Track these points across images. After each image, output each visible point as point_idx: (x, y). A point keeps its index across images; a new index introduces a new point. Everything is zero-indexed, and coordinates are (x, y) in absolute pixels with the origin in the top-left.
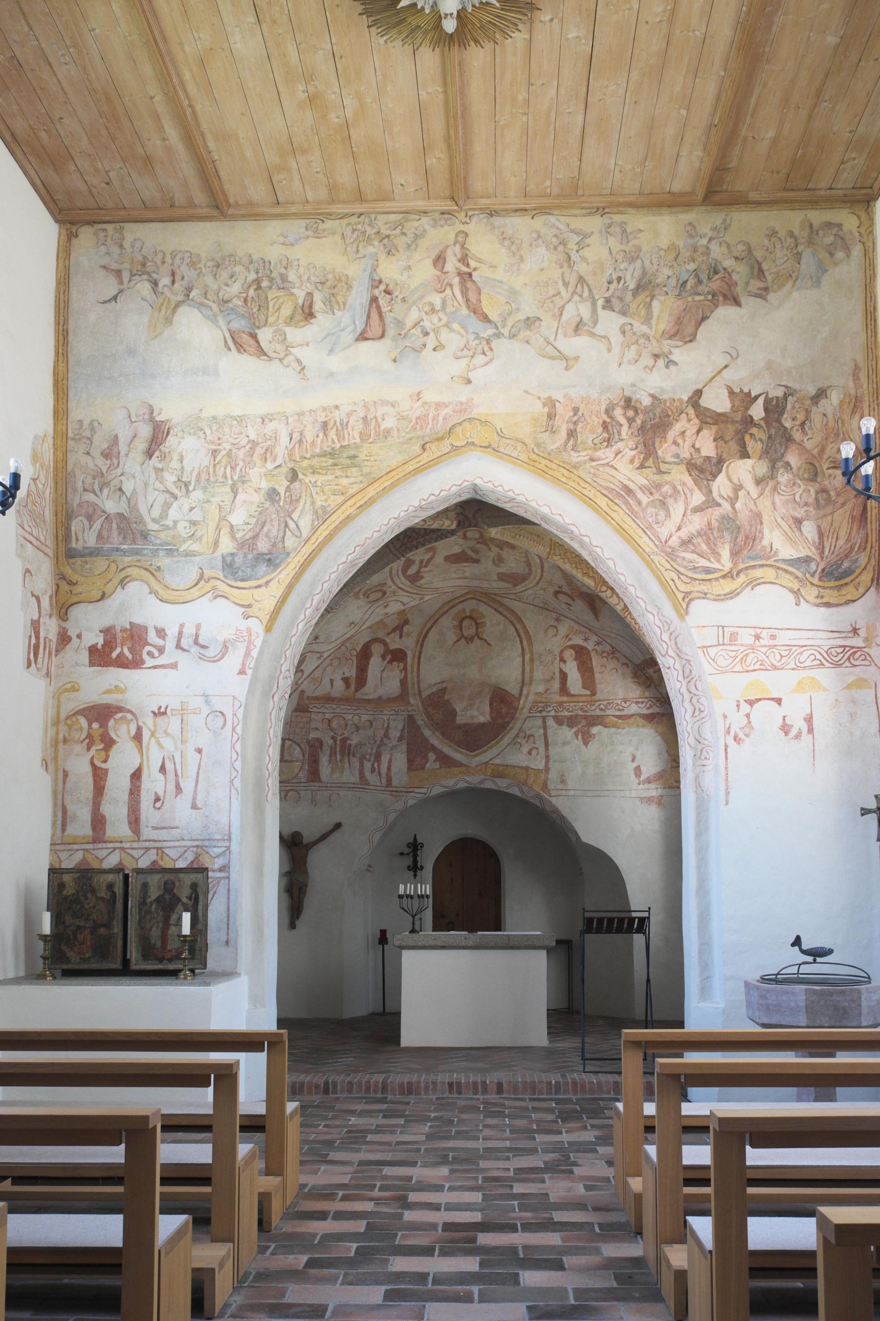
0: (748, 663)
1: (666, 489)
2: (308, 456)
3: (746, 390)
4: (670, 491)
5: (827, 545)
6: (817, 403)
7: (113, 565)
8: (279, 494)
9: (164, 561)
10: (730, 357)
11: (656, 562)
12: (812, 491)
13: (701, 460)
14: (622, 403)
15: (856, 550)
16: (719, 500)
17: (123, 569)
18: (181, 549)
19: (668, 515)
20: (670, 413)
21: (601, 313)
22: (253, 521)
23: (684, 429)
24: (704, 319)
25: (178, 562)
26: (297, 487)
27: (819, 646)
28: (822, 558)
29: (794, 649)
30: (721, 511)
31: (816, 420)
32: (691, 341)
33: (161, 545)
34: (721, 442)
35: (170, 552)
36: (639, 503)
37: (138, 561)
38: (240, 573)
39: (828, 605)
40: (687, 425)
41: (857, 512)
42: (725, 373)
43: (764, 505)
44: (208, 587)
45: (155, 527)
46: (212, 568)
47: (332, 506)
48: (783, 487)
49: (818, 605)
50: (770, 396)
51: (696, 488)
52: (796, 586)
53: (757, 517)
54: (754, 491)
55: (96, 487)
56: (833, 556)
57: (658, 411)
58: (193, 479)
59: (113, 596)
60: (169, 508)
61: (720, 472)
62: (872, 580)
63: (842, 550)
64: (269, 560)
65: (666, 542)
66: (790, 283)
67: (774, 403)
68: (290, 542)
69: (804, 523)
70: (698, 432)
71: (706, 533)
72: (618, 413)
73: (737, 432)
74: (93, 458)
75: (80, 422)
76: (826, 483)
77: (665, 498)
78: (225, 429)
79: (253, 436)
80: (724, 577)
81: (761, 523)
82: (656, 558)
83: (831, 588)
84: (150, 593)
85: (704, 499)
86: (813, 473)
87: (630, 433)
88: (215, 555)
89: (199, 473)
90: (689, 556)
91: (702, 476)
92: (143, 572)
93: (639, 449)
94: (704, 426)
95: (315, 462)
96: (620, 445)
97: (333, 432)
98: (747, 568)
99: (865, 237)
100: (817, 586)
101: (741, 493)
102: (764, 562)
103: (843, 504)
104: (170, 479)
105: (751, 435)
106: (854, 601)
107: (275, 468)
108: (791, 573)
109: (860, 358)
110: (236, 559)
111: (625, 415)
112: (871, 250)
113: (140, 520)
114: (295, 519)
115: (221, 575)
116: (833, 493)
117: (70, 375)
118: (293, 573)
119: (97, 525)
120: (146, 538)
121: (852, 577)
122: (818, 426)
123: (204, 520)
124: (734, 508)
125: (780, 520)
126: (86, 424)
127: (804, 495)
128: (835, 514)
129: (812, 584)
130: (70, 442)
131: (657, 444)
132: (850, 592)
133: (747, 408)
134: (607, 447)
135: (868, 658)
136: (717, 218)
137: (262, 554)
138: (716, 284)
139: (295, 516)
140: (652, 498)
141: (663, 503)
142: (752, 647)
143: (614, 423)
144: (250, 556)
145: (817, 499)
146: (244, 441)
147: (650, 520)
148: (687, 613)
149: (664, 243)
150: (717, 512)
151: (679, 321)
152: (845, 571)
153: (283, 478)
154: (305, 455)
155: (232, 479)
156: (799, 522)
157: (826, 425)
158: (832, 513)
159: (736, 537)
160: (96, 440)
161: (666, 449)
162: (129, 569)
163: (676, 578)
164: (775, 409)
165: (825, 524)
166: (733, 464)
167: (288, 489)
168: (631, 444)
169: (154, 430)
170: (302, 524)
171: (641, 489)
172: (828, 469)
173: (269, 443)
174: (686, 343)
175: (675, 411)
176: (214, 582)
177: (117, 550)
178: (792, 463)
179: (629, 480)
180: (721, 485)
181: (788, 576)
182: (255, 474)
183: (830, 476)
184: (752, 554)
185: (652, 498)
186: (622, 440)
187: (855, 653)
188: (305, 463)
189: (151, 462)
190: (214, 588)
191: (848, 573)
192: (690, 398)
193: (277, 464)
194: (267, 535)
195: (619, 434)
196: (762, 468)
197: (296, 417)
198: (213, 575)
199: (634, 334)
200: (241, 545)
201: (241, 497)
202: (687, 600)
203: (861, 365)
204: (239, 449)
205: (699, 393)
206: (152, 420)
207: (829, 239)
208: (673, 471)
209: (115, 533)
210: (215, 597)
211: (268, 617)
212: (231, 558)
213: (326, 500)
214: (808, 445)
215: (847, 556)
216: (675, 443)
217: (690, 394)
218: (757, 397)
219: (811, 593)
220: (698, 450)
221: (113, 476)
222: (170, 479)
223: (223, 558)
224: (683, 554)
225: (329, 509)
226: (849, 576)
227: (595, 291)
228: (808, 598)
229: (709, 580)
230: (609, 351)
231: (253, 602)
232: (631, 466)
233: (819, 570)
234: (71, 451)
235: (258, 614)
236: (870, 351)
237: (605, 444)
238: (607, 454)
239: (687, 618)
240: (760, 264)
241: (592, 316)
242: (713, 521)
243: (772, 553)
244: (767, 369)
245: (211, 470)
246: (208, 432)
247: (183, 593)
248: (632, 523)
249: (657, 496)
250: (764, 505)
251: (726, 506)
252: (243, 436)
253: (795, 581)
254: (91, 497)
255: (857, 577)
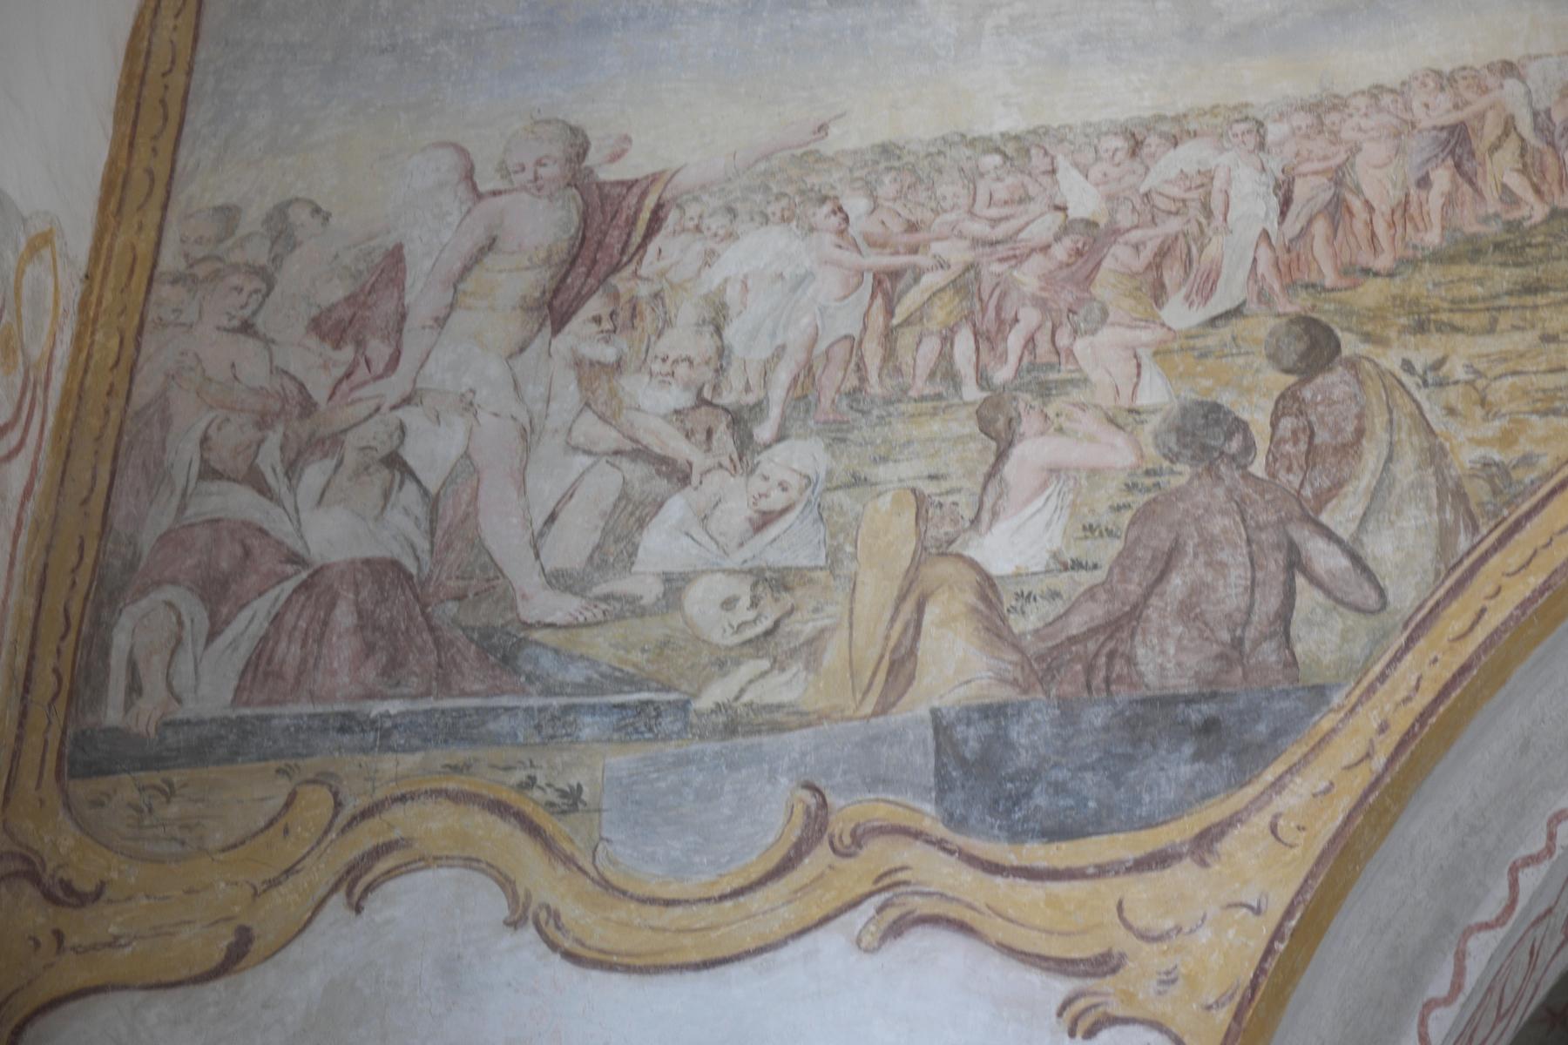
2: (1384, 262)
7: (322, 795)
8: (1242, 426)
9: (602, 764)
17: (366, 814)
18: (705, 702)
22: (1108, 551)
25: (682, 761)
26: (1337, 393)
33: (588, 687)
35: (638, 722)
37: (455, 769)
38: (1040, 799)
44: (857, 874)
45: (564, 607)
46: (878, 781)
47: (1546, 463)
55: (270, 460)
58: (778, 394)
59: (295, 950)
60: (642, 524)
64: (1209, 727)
68: (1321, 636)
74: (268, 342)
75: (228, 215)
78: (942, 190)
79: (1084, 200)
84: (514, 924)
88: (896, 717)
89: (809, 368)
92: (481, 823)
95: (1424, 283)
97: (1509, 154)
104: (654, 402)
107: (1213, 322)
110: (1017, 733)
113: (489, 582)
114: (1344, 533)
115: (928, 815)
117: (202, 55)
118: (1360, 780)
119: (250, 623)
120: (508, 660)
123: (834, 560)
126: (252, 219)
130: (163, 291)
137: (1169, 701)
139: (1341, 516)
144: (1097, 716)
146: (1043, 227)
153: (1260, 361)
154: (1365, 258)
155: (983, 379)
160: (294, 273)
162: (398, 813)
167: (1288, 403)
169: (585, 219)
170: (1382, 549)
173: (1173, 225)
176: (881, 854)
177: (346, 723)
182: (1102, 354)
188: (1371, 293)
189: (565, 342)
190: (888, 882)
193: (1218, 304)
194: (1188, 611)
197: (1302, 120)
198: (882, 813)
200: (1045, 664)
201: (1031, 452)
204: (1018, 259)
206: (577, 176)
209: (343, 647)
210: (896, 930)
211: (1224, 1016)
212: (986, 728)
213: (1506, 439)
221: (363, 410)
222: (654, 402)
223: (940, 726)
225: (1529, 476)
231: (1121, 940)
234: (162, 324)
235: (1161, 1008)
245: (873, 353)
246: (856, 205)
247: (710, 912)
252: (1034, 208)
254: (239, 502)
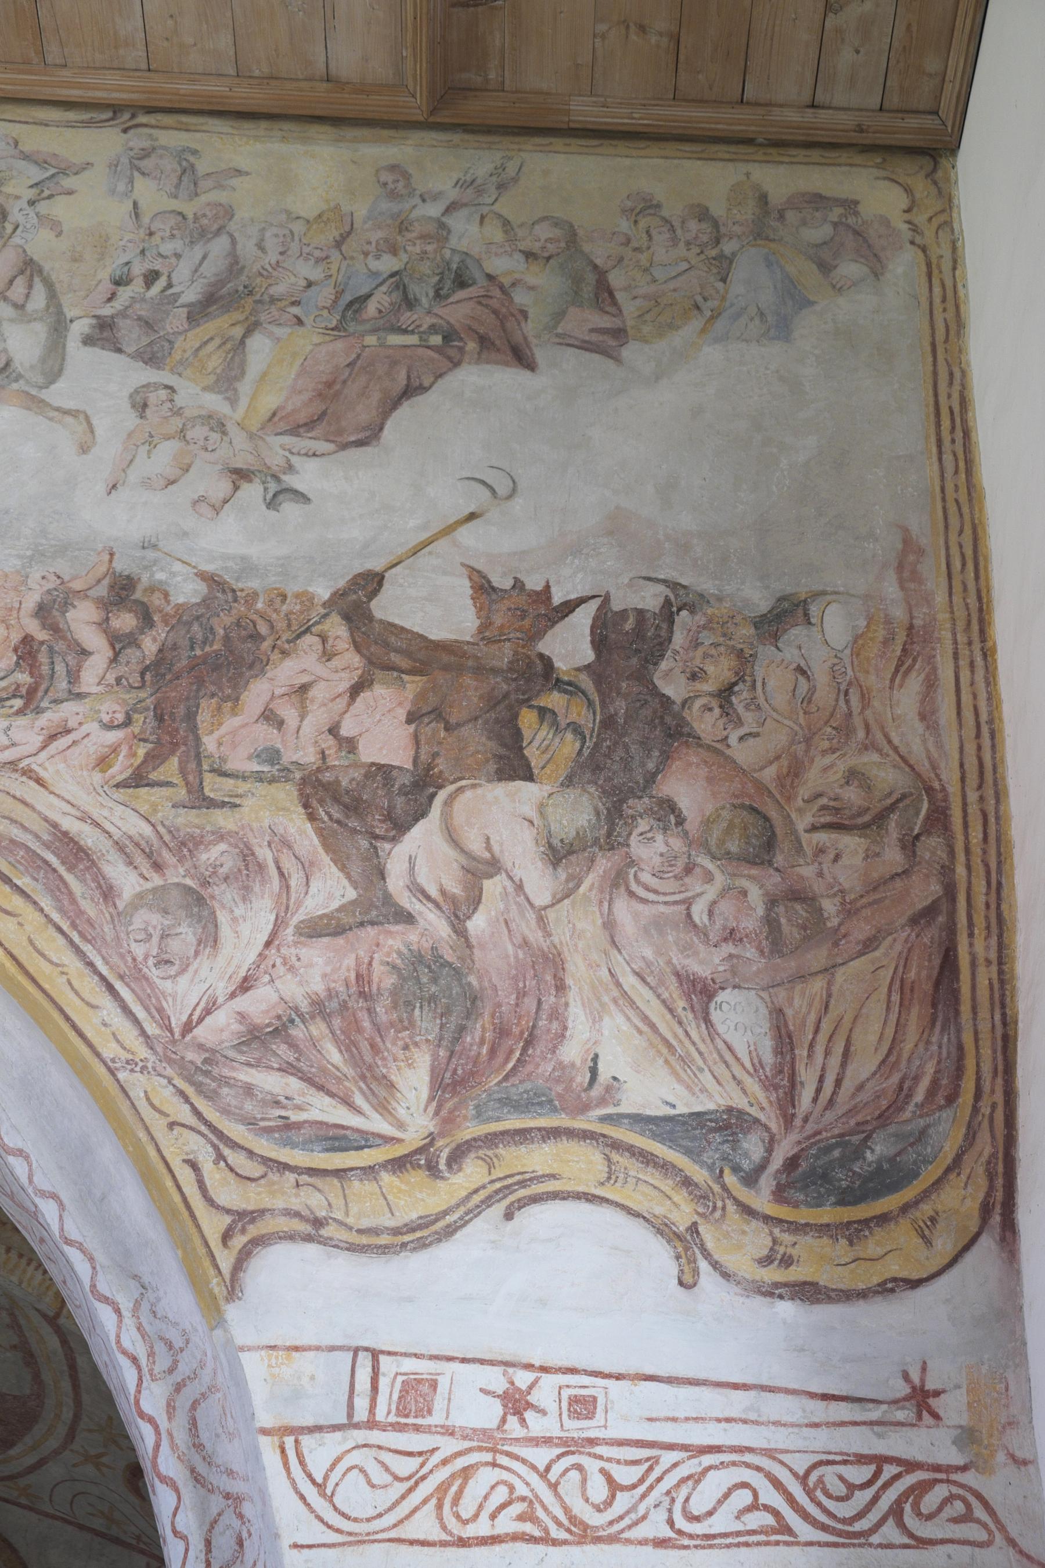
0: (467, 1509)
1: (214, 854)
3: (534, 583)
4: (229, 864)
5: (808, 1077)
6: (775, 637)
10: (487, 493)
11: (137, 1094)
12: (755, 895)
13: (357, 774)
14: (102, 590)
15: (919, 1096)
16: (407, 901)
19: (210, 939)
20: (263, 629)
21: (79, 355)
23: (305, 679)
24: (411, 391)
27: (769, 1453)
28: (788, 1120)
29: (669, 1458)
30: (413, 937)
31: (771, 684)
32: (360, 443)
34: (432, 728)
36: (108, 893)
39: (807, 1292)
40: (320, 670)
41: (921, 972)
42: (466, 535)
43: (576, 929)
48: (646, 877)
49: (771, 1292)
50: (616, 606)
51: (325, 859)
52: (682, 1212)
53: (548, 966)
54: (540, 883)
56: (830, 1116)
57: (221, 624)
61: (421, 814)
62: (986, 1210)
63: (864, 1096)
65: (188, 1027)
66: (696, 323)
67: (629, 625)
69: (722, 997)
70: (355, 691)
71: (344, 1009)
72: (82, 621)
73: (492, 702)
76: (808, 871)
77: (206, 883)
80: (399, 1164)
81: (561, 987)
82: (137, 1084)
83: (823, 1229)
85: (352, 894)
86: (760, 841)
87: (111, 678)
90: (270, 1082)
91: (353, 823)
93: (136, 728)
94: (379, 674)
96: (69, 710)
98: (492, 1140)
99: (929, 233)
100: (767, 1219)
101: (493, 887)
102: (561, 1120)
103: (869, 945)
105: (543, 712)
106: (914, 1284)
108: (665, 1167)
109: (921, 525)
111: (104, 625)
112: (946, 265)
116: (830, 907)
121: (908, 1194)
122: (780, 700)
124: (461, 932)
125: (629, 981)
127: (725, 907)
128: (840, 975)
129: (748, 1211)
131: (204, 718)
132: (897, 1250)
133: (535, 635)
134: (20, 712)
135: (979, 1512)
136: (481, 160)
138: (458, 310)
140: (157, 880)
141: (197, 902)
142: (490, 1442)
143: (60, 646)
145: (771, 923)
147: (139, 951)
148: (233, 1290)
149: (308, 202)
150: (396, 941)
151: (329, 391)
152: (879, 1171)
156: (701, 993)
157: (808, 699)
158: (828, 970)
159: (462, 1029)
161: (234, 733)
163: (206, 1158)
164: (628, 643)
165: (800, 1005)
166: (469, 794)
168: (112, 708)
171: (121, 848)
172: (814, 828)
174: (344, 446)
175: (281, 625)
178: (685, 803)
179: (84, 817)
180: (420, 857)
181: (652, 1176)
183: (821, 851)
184: (518, 1088)
185: (157, 880)
186: (80, 696)
187: (923, 1487)
191: (888, 1178)
192: (339, 595)
195: (73, 676)
196: (576, 813)
199: (178, 412)
202: (239, 1241)
203: (924, 541)
205: (372, 582)
207: (818, 233)
208: (248, 803)
214: (742, 754)
215: (883, 1119)
216: (269, 716)
217: (341, 583)
218: (569, 607)
219: (742, 1245)
220: (350, 745)
224: (246, 1075)
226: (894, 1187)
227: (66, 300)
228: (730, 1260)
229: (340, 1173)
230: (84, 449)
232: (97, 777)
233: (777, 1162)
236: (952, 509)
237: (18, 703)
238: (16, 735)
239: (232, 1312)
240: (601, 275)
241: (43, 360)
242: (378, 969)
243: (596, 1092)
244: (610, 533)
248: (73, 964)
249: (177, 874)
250: (576, 929)
251: (435, 924)
253: (681, 1197)
255: (925, 1195)
